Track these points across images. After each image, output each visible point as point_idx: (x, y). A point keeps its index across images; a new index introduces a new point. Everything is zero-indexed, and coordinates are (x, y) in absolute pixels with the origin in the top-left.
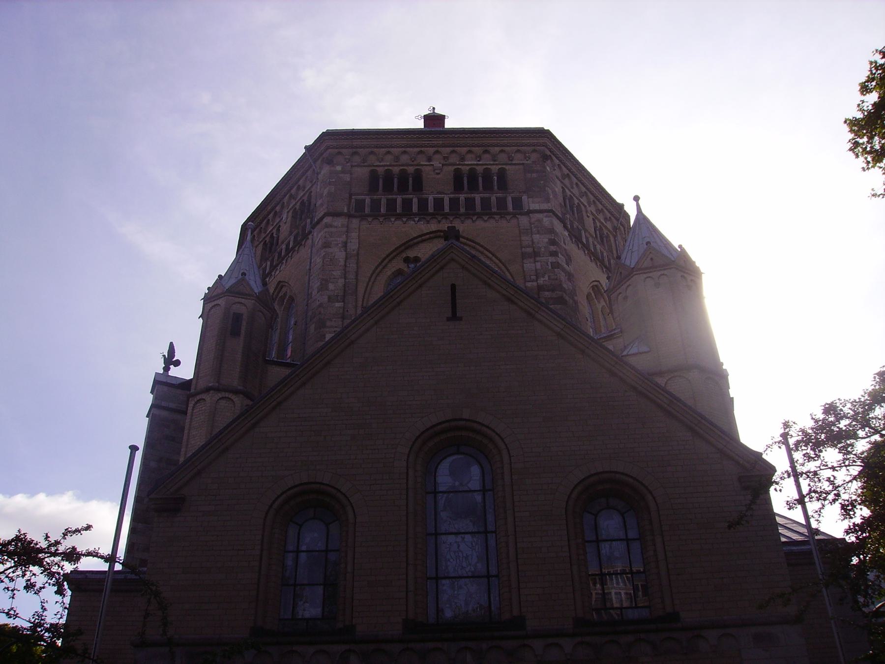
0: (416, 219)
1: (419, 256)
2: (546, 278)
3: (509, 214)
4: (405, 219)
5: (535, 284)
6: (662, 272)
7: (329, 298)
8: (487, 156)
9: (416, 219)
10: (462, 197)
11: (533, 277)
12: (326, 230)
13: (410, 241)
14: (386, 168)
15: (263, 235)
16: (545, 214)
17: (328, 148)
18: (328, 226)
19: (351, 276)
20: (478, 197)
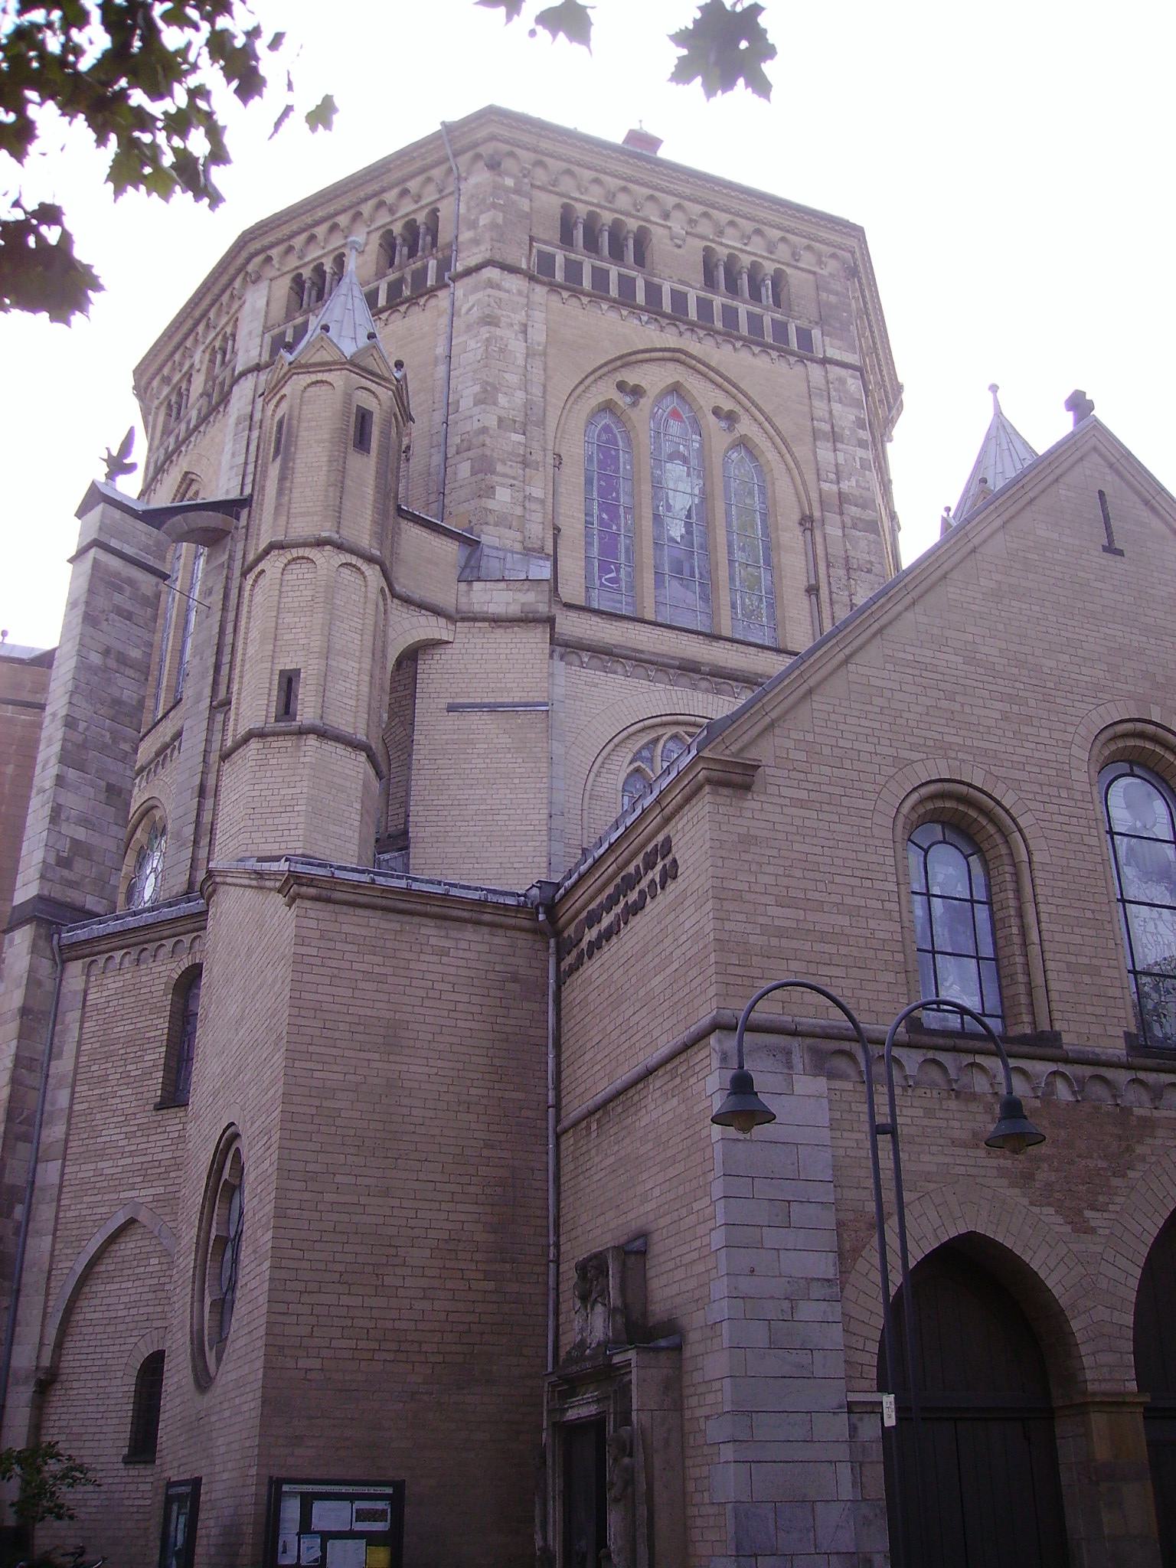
1: (643, 385)
7: (500, 420)
11: (832, 476)
12: (489, 291)
13: (630, 354)
15: (293, 262)
17: (493, 138)
18: (491, 284)
19: (537, 391)
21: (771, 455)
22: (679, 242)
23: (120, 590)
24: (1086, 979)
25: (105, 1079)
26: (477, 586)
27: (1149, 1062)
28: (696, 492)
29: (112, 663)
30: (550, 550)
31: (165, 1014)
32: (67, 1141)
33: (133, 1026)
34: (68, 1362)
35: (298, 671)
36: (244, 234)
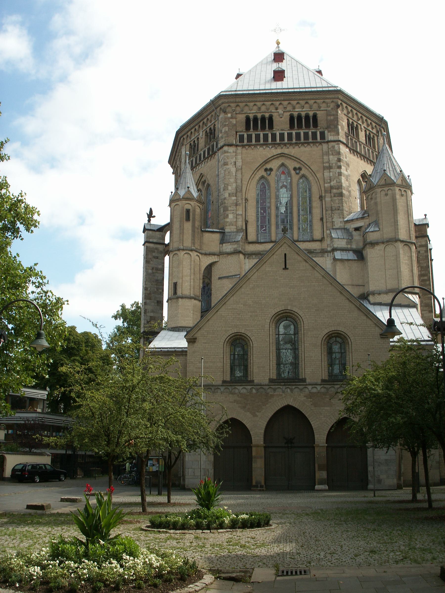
0: (270, 147)
2: (335, 181)
3: (318, 142)
4: (264, 147)
5: (329, 185)
6: (389, 188)
7: (229, 194)
8: (307, 105)
9: (270, 147)
10: (294, 132)
11: (329, 181)
14: (254, 114)
15: (189, 140)
16: (336, 143)
17: (223, 103)
18: (226, 152)
19: (239, 181)
20: (302, 132)
21: (311, 178)
22: (281, 116)
23: (154, 252)
24: (262, 369)
26: (224, 245)
27: (273, 384)
28: (289, 196)
29: (154, 271)
30: (244, 228)
35: (177, 282)
36: (178, 133)
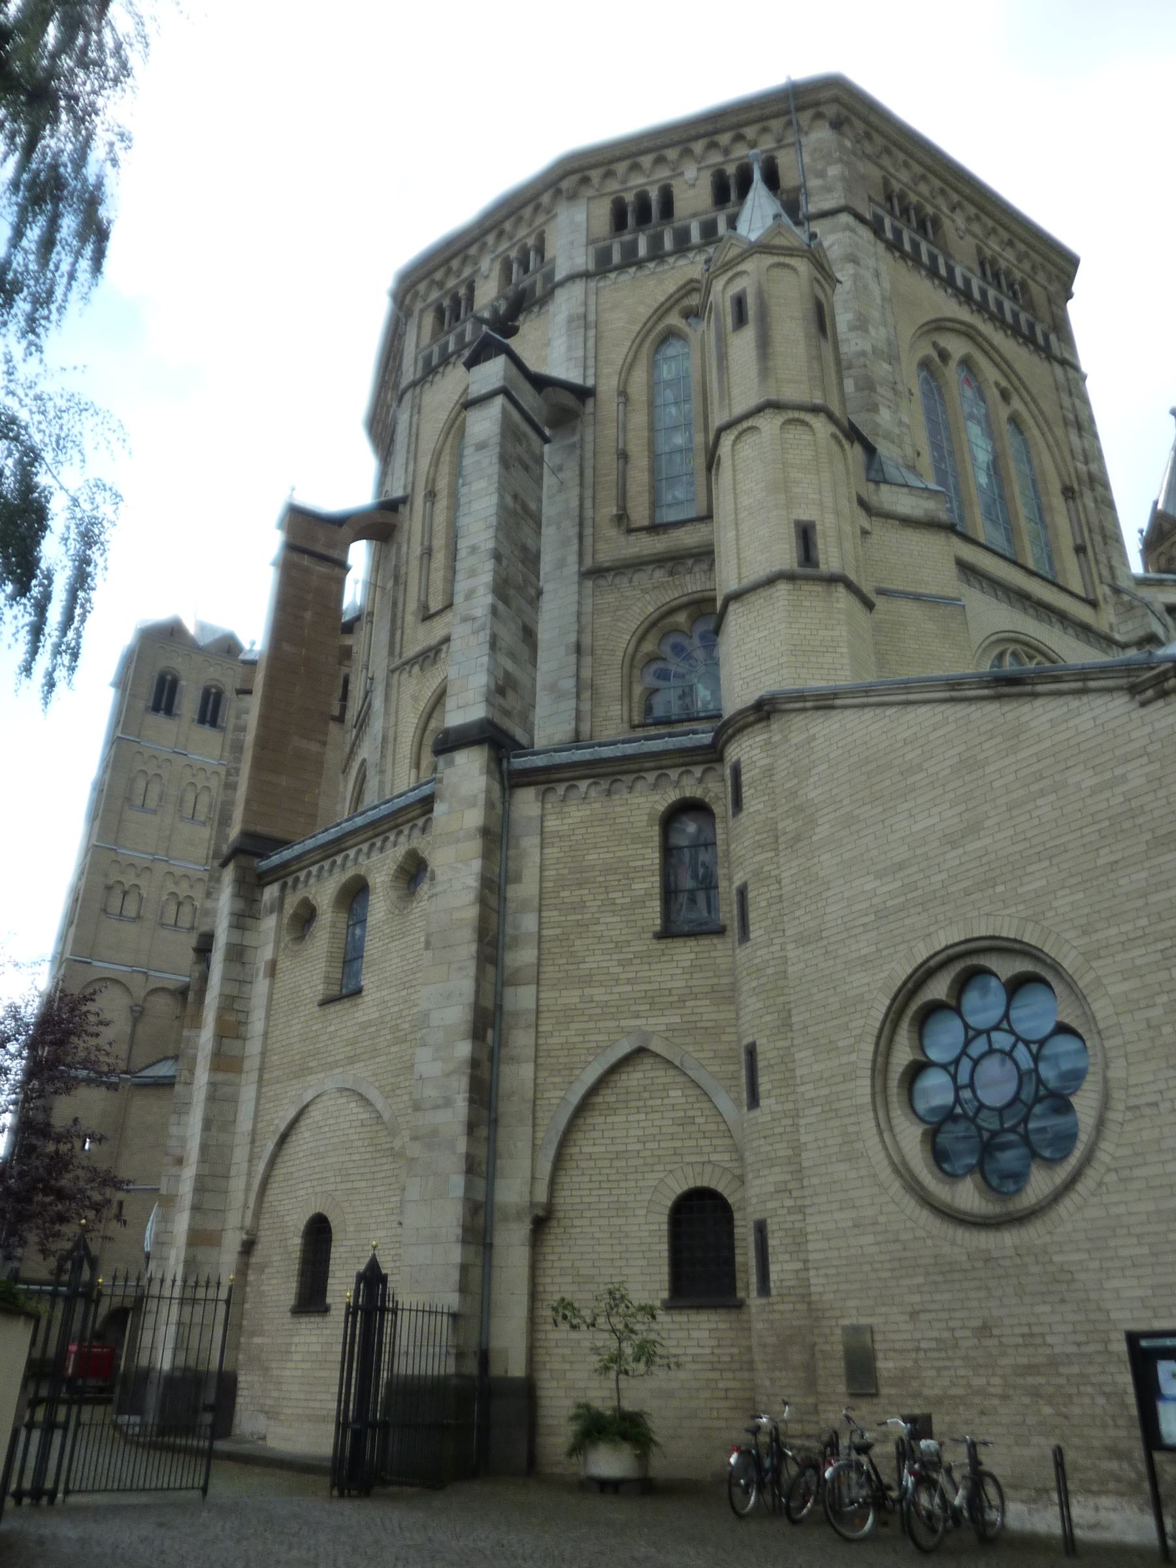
25: (582, 906)
29: (518, 508)
31: (652, 844)
32: (539, 965)
33: (611, 855)
34: (565, 1199)
